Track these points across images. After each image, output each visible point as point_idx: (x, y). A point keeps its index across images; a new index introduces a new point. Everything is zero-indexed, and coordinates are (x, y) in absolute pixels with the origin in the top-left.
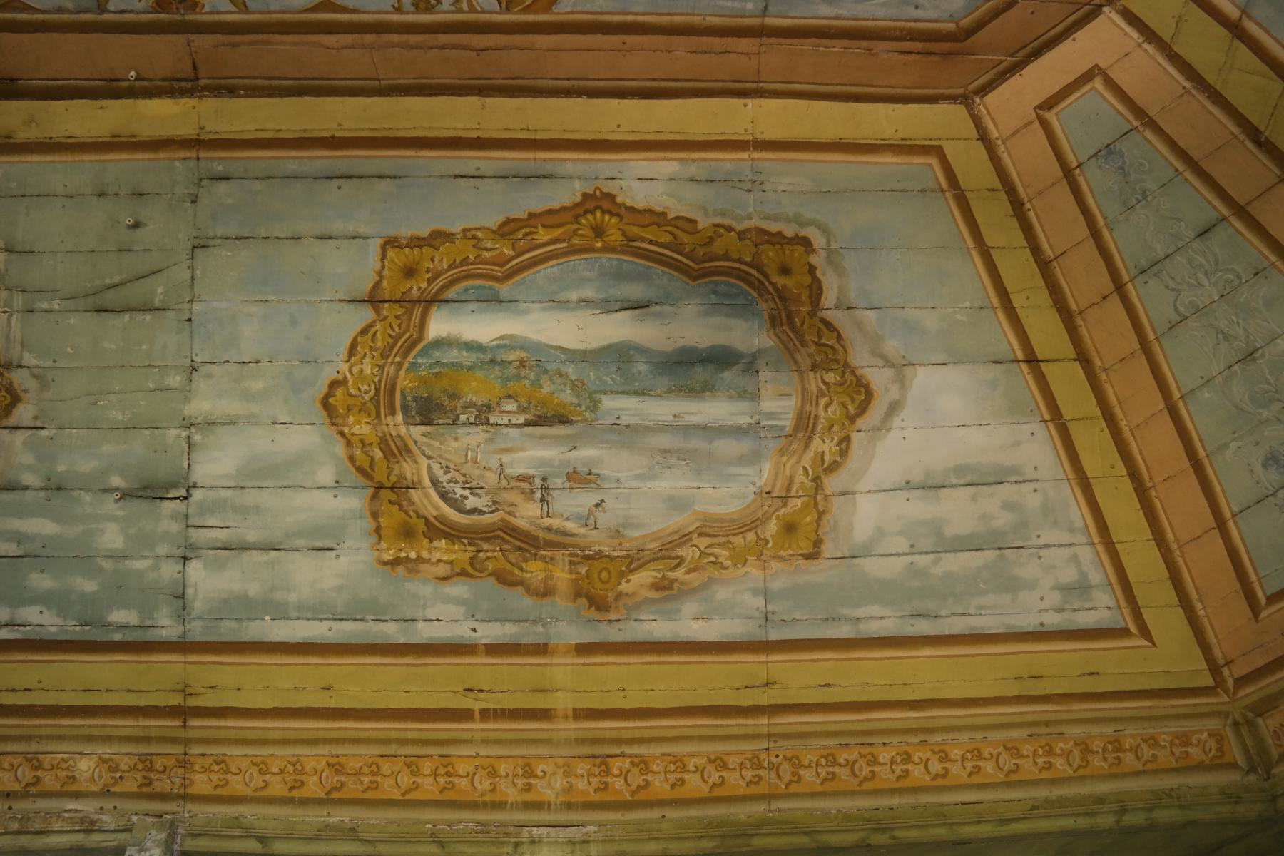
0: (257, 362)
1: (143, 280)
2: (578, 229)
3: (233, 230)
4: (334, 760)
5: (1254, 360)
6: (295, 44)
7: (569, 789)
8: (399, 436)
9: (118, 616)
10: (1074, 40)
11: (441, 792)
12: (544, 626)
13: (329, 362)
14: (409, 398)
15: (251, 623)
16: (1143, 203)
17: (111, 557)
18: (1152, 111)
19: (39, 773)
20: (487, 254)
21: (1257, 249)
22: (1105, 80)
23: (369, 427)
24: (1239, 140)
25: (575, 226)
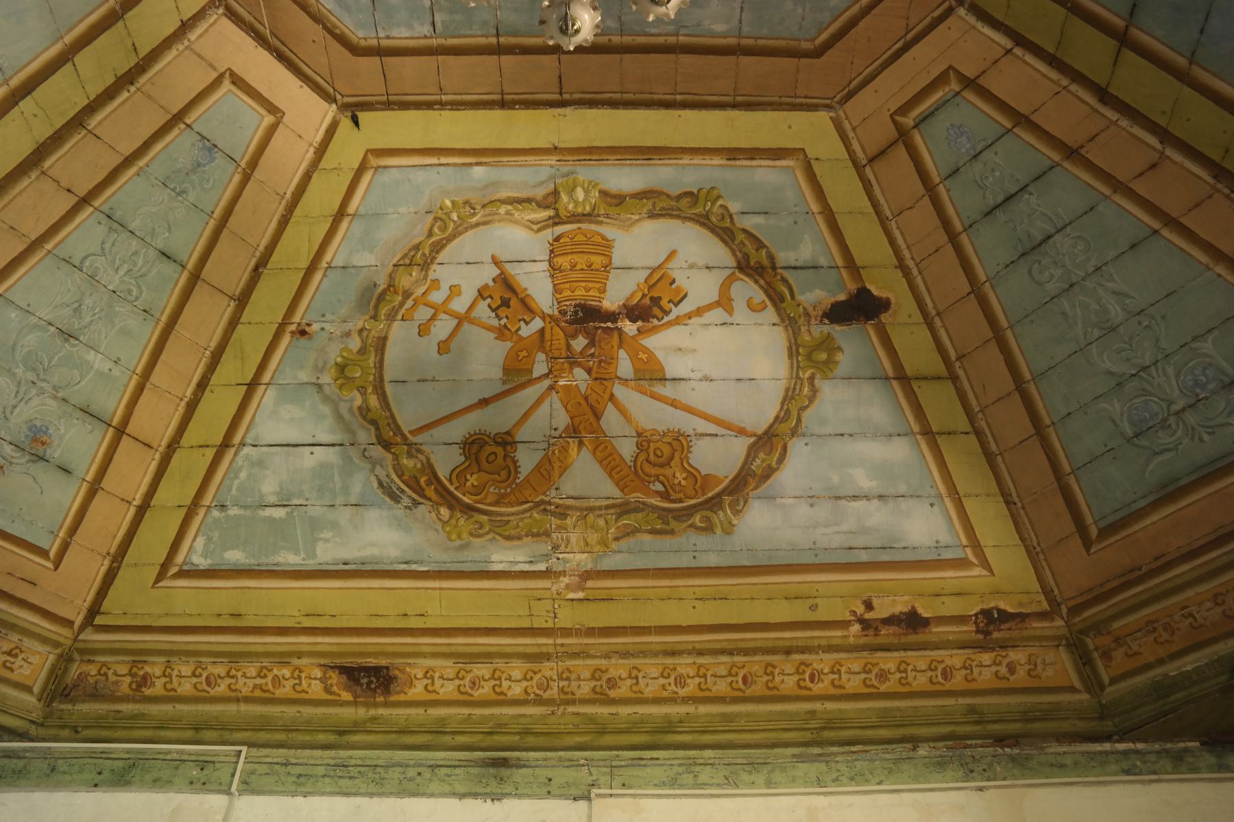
5: (66, 340)
10: (301, 87)
16: (174, 194)
18: (257, 174)
21: (168, 301)
22: (273, 125)
24: (255, 252)
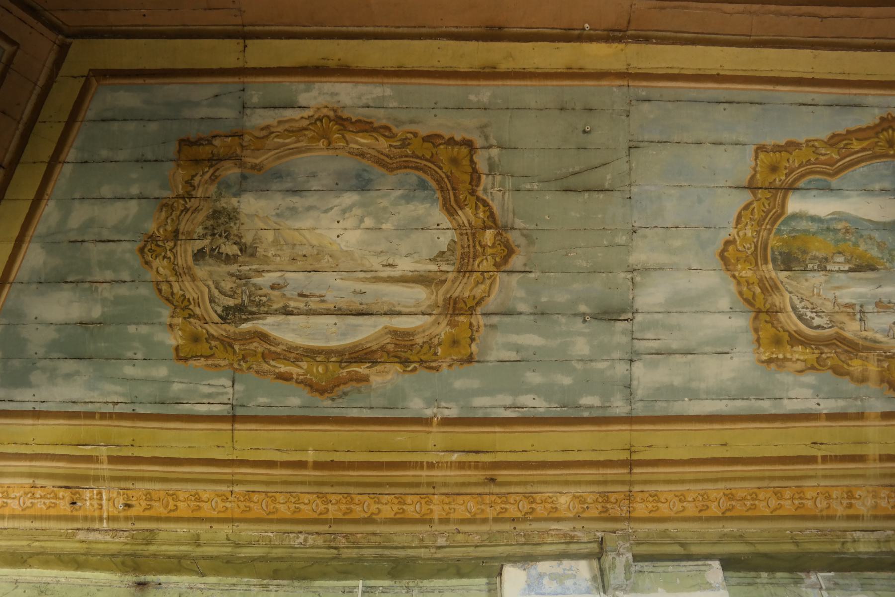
0: (676, 228)
1: (596, 169)
2: (878, 142)
3: (657, 137)
4: (727, 492)
6: (704, 9)
7: (875, 507)
8: (771, 278)
9: (587, 400)
11: (796, 510)
12: (861, 401)
13: (724, 228)
14: (776, 253)
15: (675, 403)
17: (582, 360)
19: (533, 506)
20: (823, 158)
23: (752, 272)
25: (876, 140)
